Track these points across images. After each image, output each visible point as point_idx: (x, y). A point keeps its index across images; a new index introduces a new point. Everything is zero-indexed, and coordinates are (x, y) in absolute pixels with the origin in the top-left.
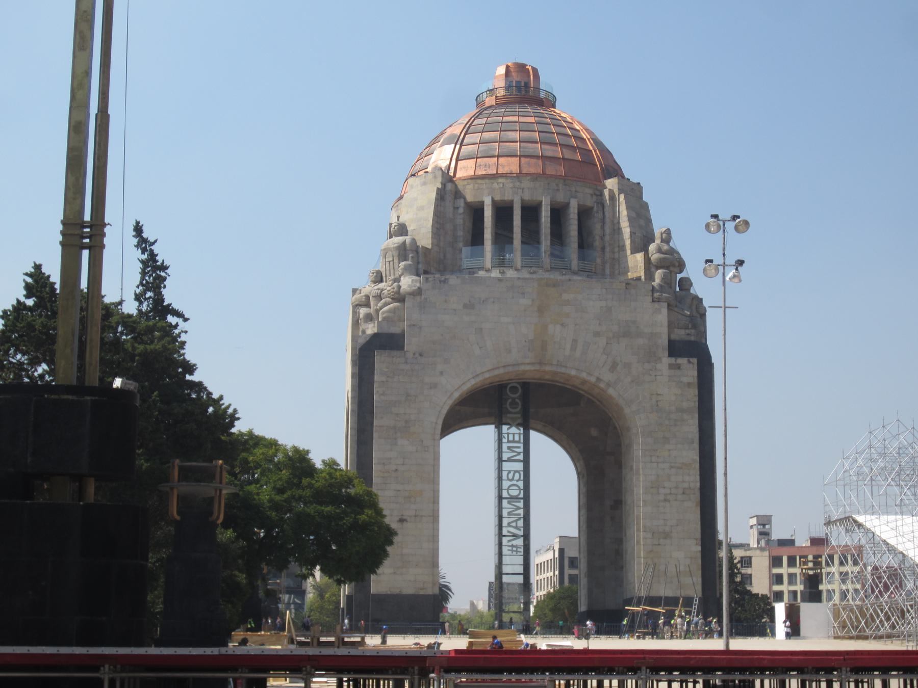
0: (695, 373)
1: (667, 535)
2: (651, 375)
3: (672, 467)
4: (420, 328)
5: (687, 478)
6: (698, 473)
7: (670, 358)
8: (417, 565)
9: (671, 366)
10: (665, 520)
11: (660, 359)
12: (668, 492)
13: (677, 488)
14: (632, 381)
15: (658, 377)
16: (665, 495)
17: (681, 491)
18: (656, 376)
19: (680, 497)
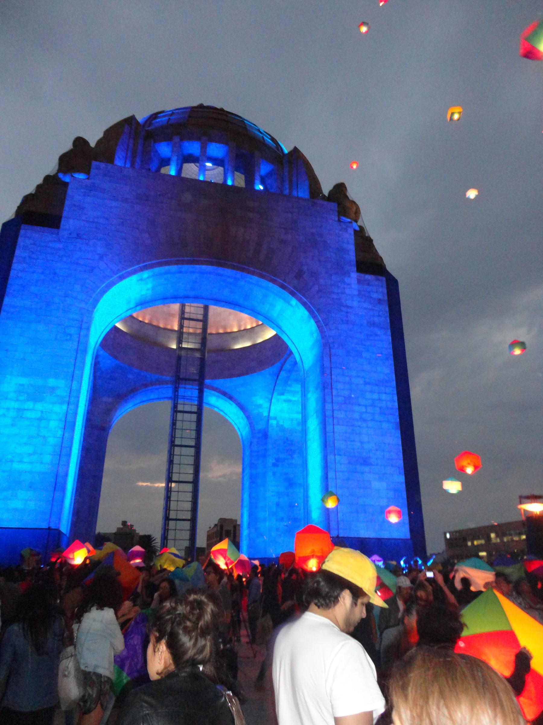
0: (385, 291)
1: (366, 462)
2: (338, 287)
3: (366, 383)
4: (83, 209)
5: (383, 397)
6: (395, 392)
7: (358, 274)
8: (30, 487)
9: (359, 282)
10: (362, 443)
11: (347, 274)
12: (363, 409)
13: (373, 406)
14: (320, 291)
15: (348, 291)
16: (361, 413)
17: (377, 410)
18: (344, 288)
19: (377, 417)
